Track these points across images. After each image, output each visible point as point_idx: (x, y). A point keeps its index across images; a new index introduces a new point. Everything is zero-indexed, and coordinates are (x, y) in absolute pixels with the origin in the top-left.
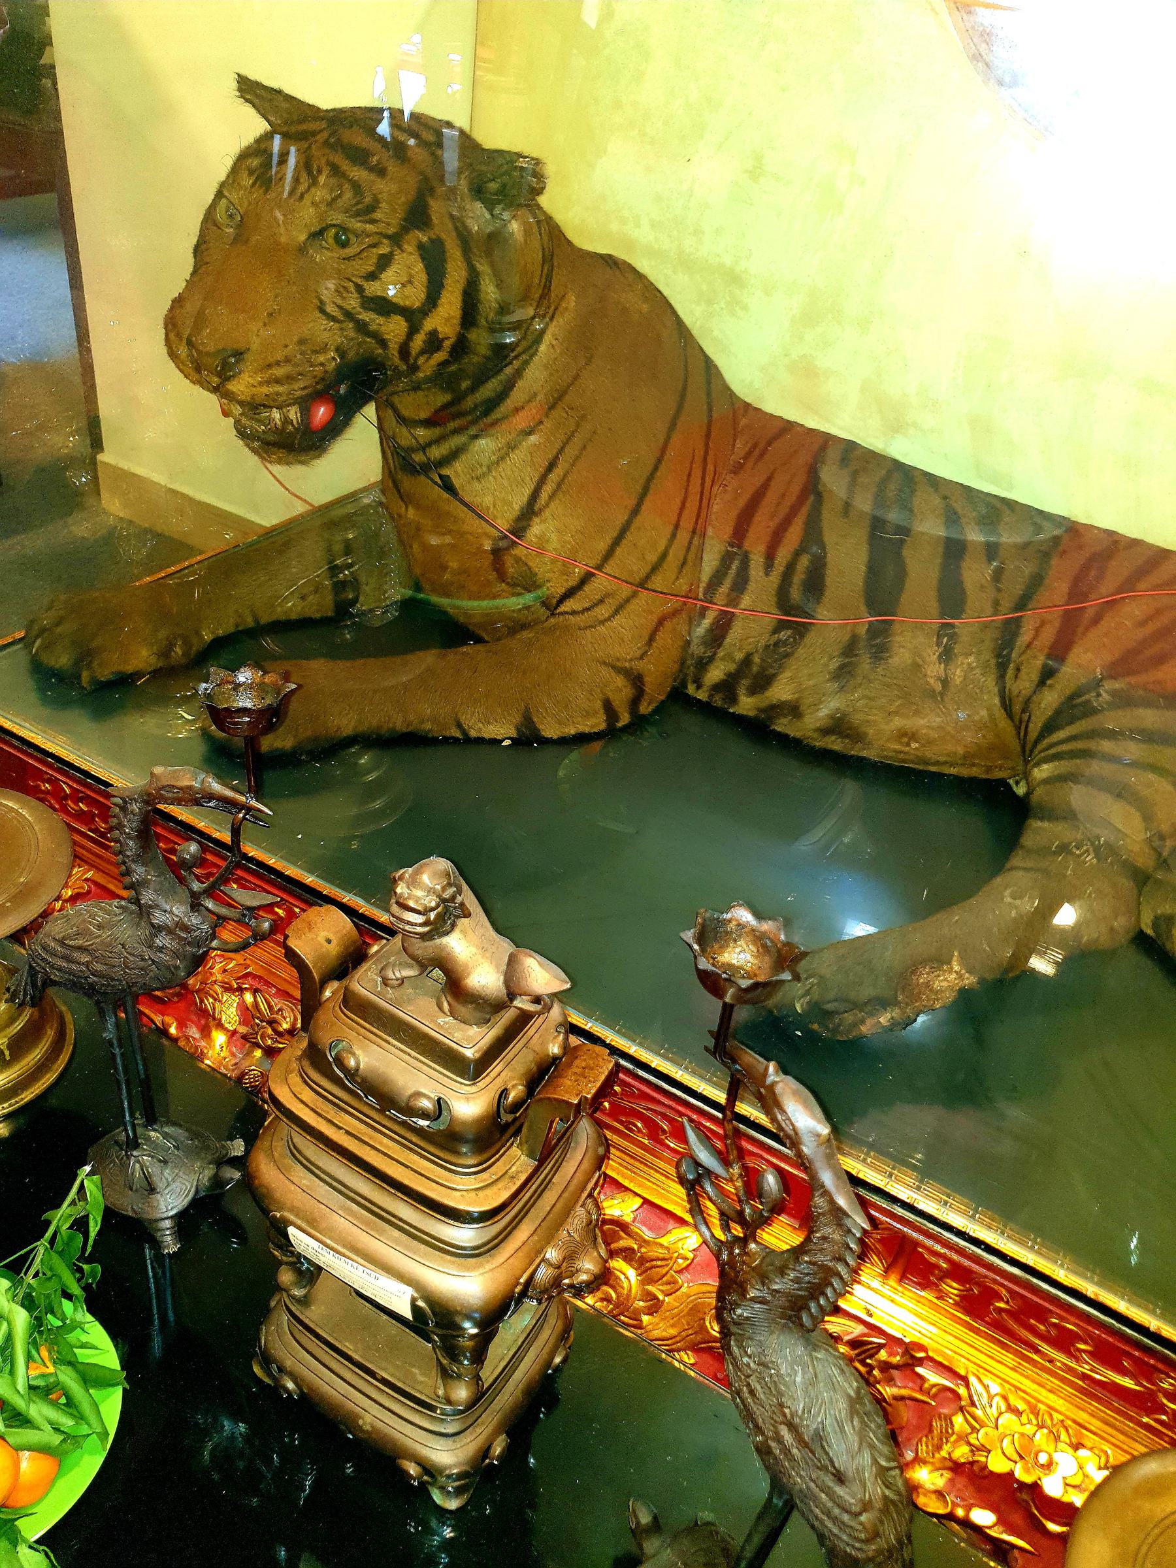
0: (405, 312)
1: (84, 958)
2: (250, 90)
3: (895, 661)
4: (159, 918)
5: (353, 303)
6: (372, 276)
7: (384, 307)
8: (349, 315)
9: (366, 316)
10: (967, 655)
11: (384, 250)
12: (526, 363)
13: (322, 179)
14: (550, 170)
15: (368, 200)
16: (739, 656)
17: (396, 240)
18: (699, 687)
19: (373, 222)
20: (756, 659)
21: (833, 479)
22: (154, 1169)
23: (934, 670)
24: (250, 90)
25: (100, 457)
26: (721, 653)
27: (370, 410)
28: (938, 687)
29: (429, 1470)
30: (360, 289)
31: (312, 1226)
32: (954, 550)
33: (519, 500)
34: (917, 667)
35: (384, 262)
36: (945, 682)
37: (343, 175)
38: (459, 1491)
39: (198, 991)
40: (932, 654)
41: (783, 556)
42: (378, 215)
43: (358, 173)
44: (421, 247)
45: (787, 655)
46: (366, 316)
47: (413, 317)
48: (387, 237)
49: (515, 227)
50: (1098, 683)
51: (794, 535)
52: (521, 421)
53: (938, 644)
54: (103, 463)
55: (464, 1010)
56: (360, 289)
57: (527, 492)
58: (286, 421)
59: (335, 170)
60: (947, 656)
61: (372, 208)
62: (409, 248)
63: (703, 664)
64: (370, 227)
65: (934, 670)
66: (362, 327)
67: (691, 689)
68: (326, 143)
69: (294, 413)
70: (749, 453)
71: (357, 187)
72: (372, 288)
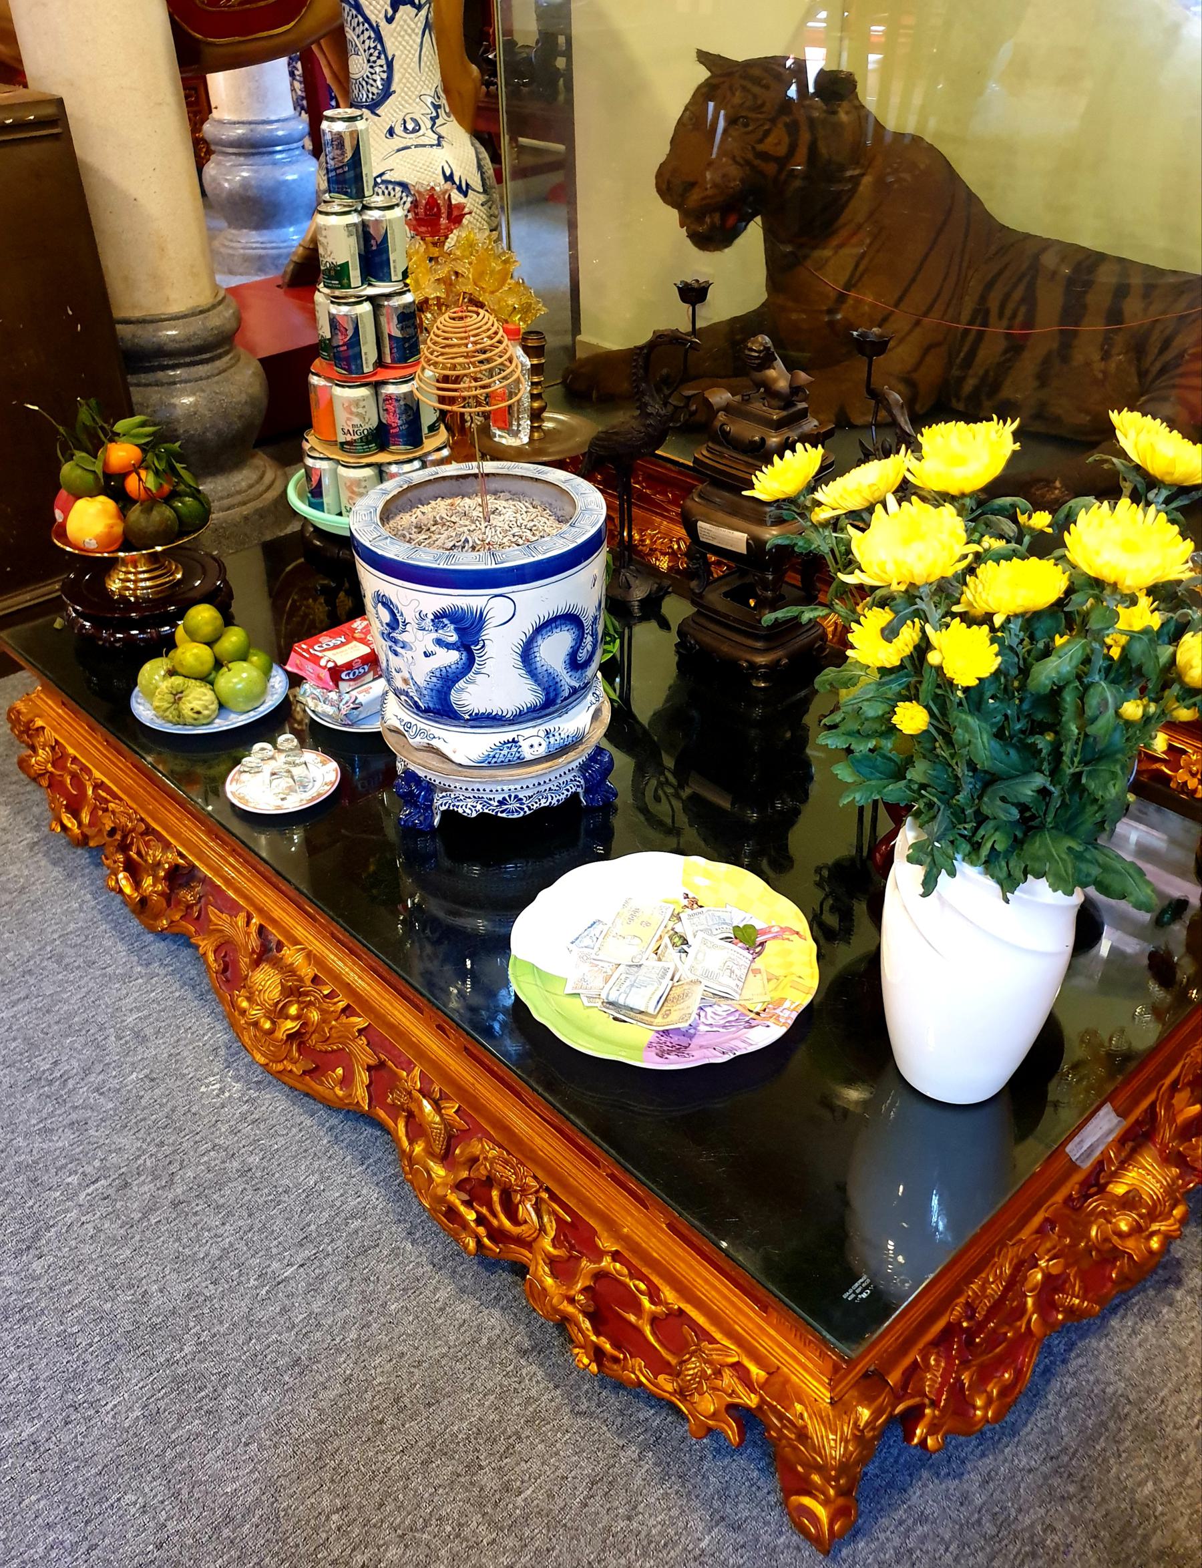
0: (776, 159)
1: (615, 437)
2: (704, 57)
3: (1075, 364)
4: (650, 410)
5: (750, 156)
6: (761, 141)
7: (764, 156)
8: (748, 163)
9: (757, 162)
10: (1119, 354)
11: (766, 127)
12: (850, 198)
13: (738, 94)
14: (857, 78)
15: (759, 102)
16: (981, 372)
17: (773, 121)
18: (958, 400)
19: (761, 113)
20: (991, 373)
21: (1049, 260)
22: (631, 580)
23: (1098, 366)
24: (704, 57)
25: (579, 338)
26: (971, 372)
27: (758, 219)
28: (1100, 376)
29: (752, 665)
30: (753, 148)
31: (707, 520)
32: (1121, 291)
33: (843, 279)
34: (1088, 364)
35: (767, 133)
36: (1104, 372)
37: (749, 91)
38: (765, 678)
39: (648, 555)
40: (1096, 357)
41: (1010, 307)
42: (764, 109)
43: (756, 90)
44: (786, 125)
45: (1010, 368)
46: (757, 162)
47: (783, 162)
48: (769, 120)
49: (843, 117)
50: (1185, 351)
51: (1018, 294)
52: (844, 233)
53: (1102, 349)
54: (580, 341)
55: (775, 403)
56: (753, 148)
57: (848, 273)
58: (713, 224)
59: (744, 88)
60: (1106, 356)
61: (763, 105)
62: (780, 125)
63: (961, 380)
64: (759, 116)
65: (1098, 366)
66: (752, 167)
67: (954, 404)
68: (741, 77)
69: (717, 217)
70: (997, 253)
71: (755, 97)
72: (760, 147)
